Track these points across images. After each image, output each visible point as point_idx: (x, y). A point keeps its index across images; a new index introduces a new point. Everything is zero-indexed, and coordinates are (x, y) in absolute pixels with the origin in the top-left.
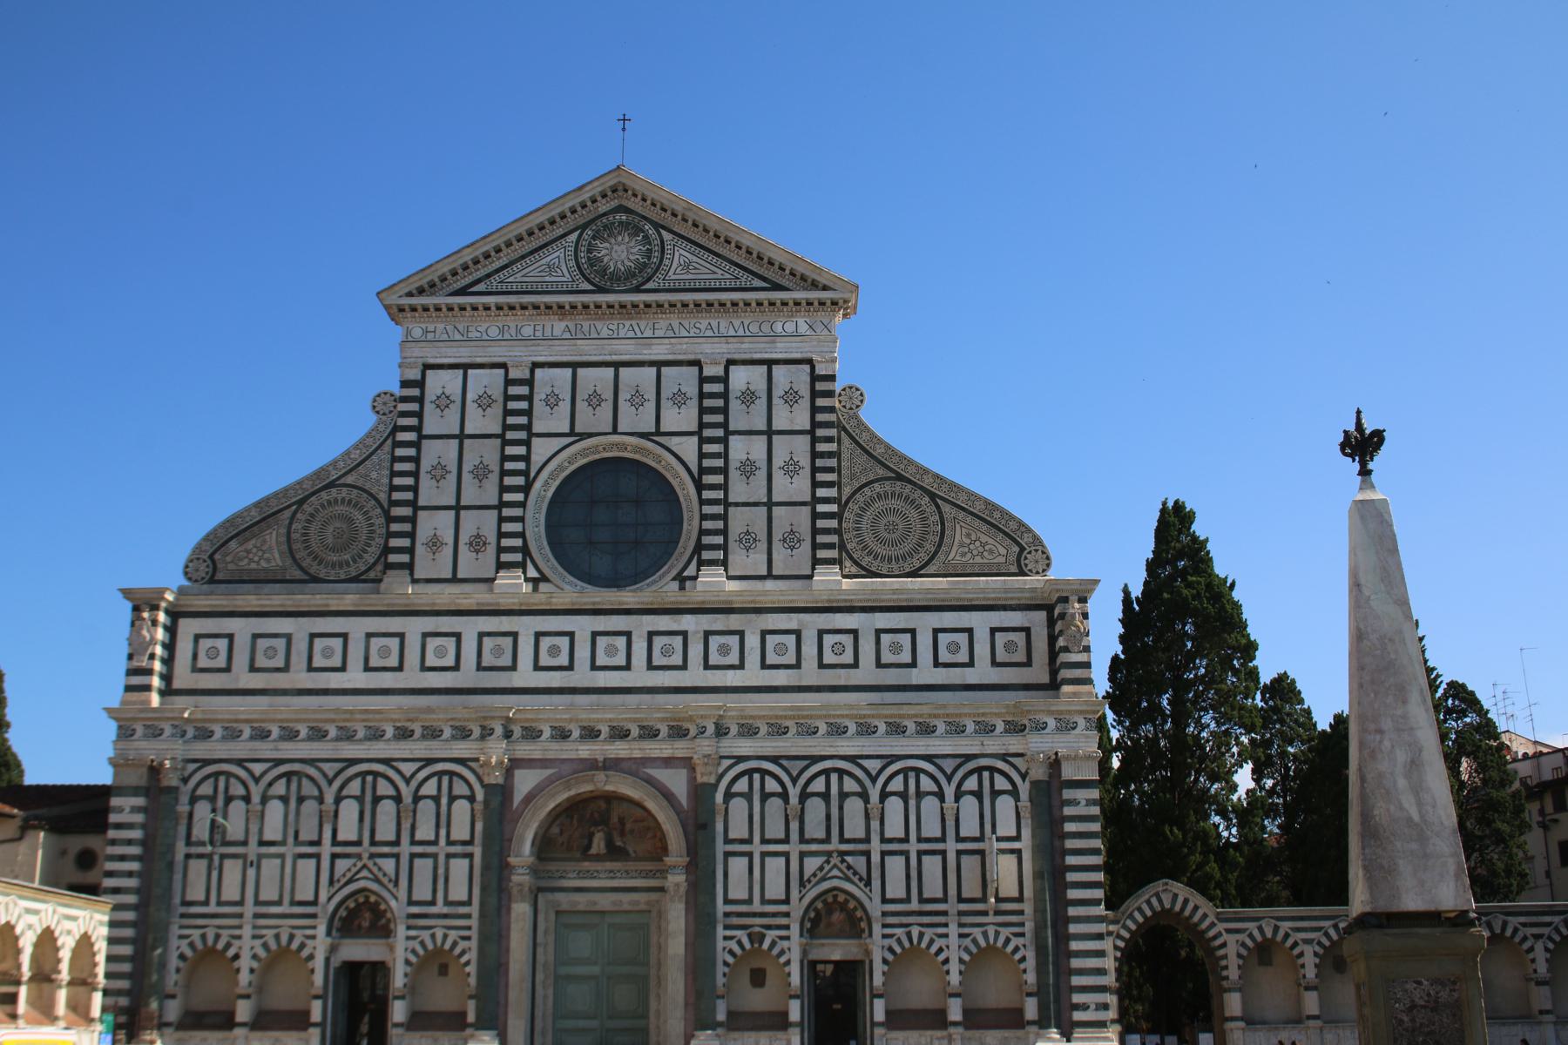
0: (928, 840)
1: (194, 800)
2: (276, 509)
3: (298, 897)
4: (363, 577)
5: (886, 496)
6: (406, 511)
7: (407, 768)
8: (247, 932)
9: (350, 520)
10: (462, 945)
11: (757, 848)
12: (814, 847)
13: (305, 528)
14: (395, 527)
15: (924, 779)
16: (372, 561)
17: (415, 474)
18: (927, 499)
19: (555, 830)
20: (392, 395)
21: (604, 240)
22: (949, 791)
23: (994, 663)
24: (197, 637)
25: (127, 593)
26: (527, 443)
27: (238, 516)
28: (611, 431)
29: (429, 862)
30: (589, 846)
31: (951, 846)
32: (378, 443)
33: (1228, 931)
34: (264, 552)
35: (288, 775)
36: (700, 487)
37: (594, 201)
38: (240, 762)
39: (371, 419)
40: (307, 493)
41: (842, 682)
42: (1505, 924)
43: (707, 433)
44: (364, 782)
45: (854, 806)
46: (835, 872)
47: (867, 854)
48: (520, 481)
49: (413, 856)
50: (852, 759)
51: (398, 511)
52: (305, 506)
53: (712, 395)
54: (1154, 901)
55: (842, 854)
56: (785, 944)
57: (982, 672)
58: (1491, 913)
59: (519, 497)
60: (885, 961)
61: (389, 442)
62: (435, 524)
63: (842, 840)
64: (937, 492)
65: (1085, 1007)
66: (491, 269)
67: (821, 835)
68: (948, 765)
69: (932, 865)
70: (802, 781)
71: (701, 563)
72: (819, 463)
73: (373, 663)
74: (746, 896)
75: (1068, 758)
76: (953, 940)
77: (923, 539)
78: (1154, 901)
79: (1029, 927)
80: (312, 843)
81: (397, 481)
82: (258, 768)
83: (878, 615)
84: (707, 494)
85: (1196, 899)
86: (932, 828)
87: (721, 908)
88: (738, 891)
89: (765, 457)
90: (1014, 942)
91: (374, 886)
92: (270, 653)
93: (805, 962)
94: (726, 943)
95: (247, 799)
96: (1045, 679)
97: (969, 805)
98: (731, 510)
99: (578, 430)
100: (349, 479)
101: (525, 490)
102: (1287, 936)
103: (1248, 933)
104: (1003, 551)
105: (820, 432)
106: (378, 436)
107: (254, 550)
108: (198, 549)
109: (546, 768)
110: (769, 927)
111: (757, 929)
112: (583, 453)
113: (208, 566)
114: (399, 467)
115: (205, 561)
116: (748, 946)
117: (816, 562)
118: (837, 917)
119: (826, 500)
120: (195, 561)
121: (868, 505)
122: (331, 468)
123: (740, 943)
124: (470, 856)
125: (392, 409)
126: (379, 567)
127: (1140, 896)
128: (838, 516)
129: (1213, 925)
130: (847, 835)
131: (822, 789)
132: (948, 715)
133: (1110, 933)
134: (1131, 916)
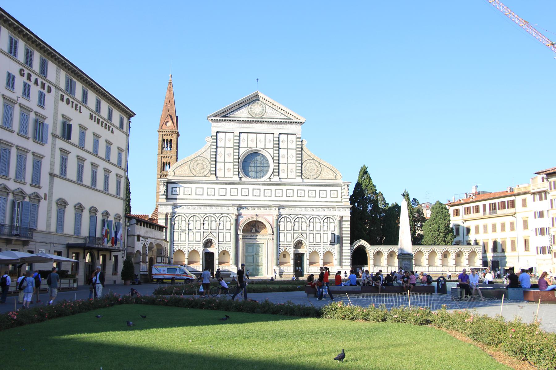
0: (318, 231)
3: (196, 240)
7: (218, 215)
9: (202, 164)
10: (229, 249)
11: (285, 232)
12: (296, 232)
13: (193, 165)
14: (212, 166)
19: (245, 227)
21: (253, 106)
22: (322, 222)
24: (172, 188)
29: (223, 233)
30: (252, 231)
31: (322, 232)
33: (372, 249)
38: (184, 213)
43: (275, 149)
44: (209, 218)
45: (304, 224)
46: (300, 237)
47: (306, 233)
50: (304, 215)
51: (212, 163)
53: (276, 141)
60: (309, 253)
63: (302, 231)
66: (230, 112)
67: (298, 230)
68: (322, 217)
69: (318, 235)
72: (297, 156)
73: (209, 194)
74: (283, 241)
80: (199, 230)
81: (212, 156)
82: (187, 215)
84: (275, 161)
85: (366, 243)
86: (318, 229)
88: (282, 239)
90: (333, 250)
92: (188, 191)
95: (185, 221)
96: (340, 201)
97: (325, 224)
98: (280, 165)
99: (249, 147)
100: (202, 155)
101: (239, 159)
102: (382, 250)
105: (297, 149)
110: (288, 247)
112: (249, 151)
118: (300, 245)
119: (298, 163)
121: (307, 164)
124: (230, 232)
126: (209, 174)
130: (302, 230)
131: (298, 221)
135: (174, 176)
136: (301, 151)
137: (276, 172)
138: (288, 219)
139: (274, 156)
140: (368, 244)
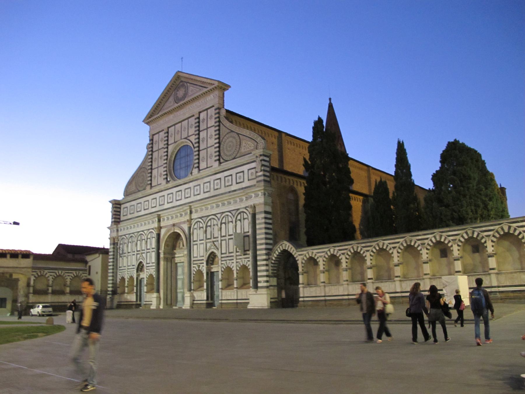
1: (120, 244)
5: (229, 138)
8: (126, 273)
9: (143, 176)
15: (230, 218)
17: (152, 162)
18: (237, 135)
21: (178, 91)
23: (249, 180)
25: (110, 202)
26: (167, 148)
27: (130, 180)
28: (180, 139)
33: (300, 255)
35: (131, 237)
36: (194, 148)
37: (175, 82)
38: (125, 235)
41: (218, 193)
42: (384, 244)
46: (212, 247)
47: (218, 241)
48: (166, 157)
49: (147, 252)
50: (214, 215)
54: (281, 247)
55: (213, 242)
56: (203, 267)
57: (246, 184)
58: (378, 241)
59: (165, 161)
62: (155, 172)
64: (239, 133)
65: (260, 282)
70: (206, 223)
71: (195, 168)
75: (257, 205)
76: (234, 264)
77: (236, 147)
78: (281, 247)
79: (251, 258)
82: (127, 236)
83: (225, 172)
85: (291, 246)
87: (192, 259)
89: (206, 135)
90: (249, 263)
91: (141, 260)
93: (209, 273)
94: (194, 268)
97: (238, 222)
98: (201, 152)
99: (176, 141)
100: (143, 167)
102: (316, 255)
103: (304, 255)
104: (253, 145)
109: (165, 228)
111: (199, 264)
116: (197, 269)
117: (216, 161)
121: (225, 141)
123: (196, 268)
127: (277, 246)
128: (219, 147)
129: (295, 253)
132: (233, 198)
133: (269, 259)
134: (275, 252)
136: (219, 126)
137: (196, 163)
138: (200, 223)
139: (196, 143)
140: (293, 248)
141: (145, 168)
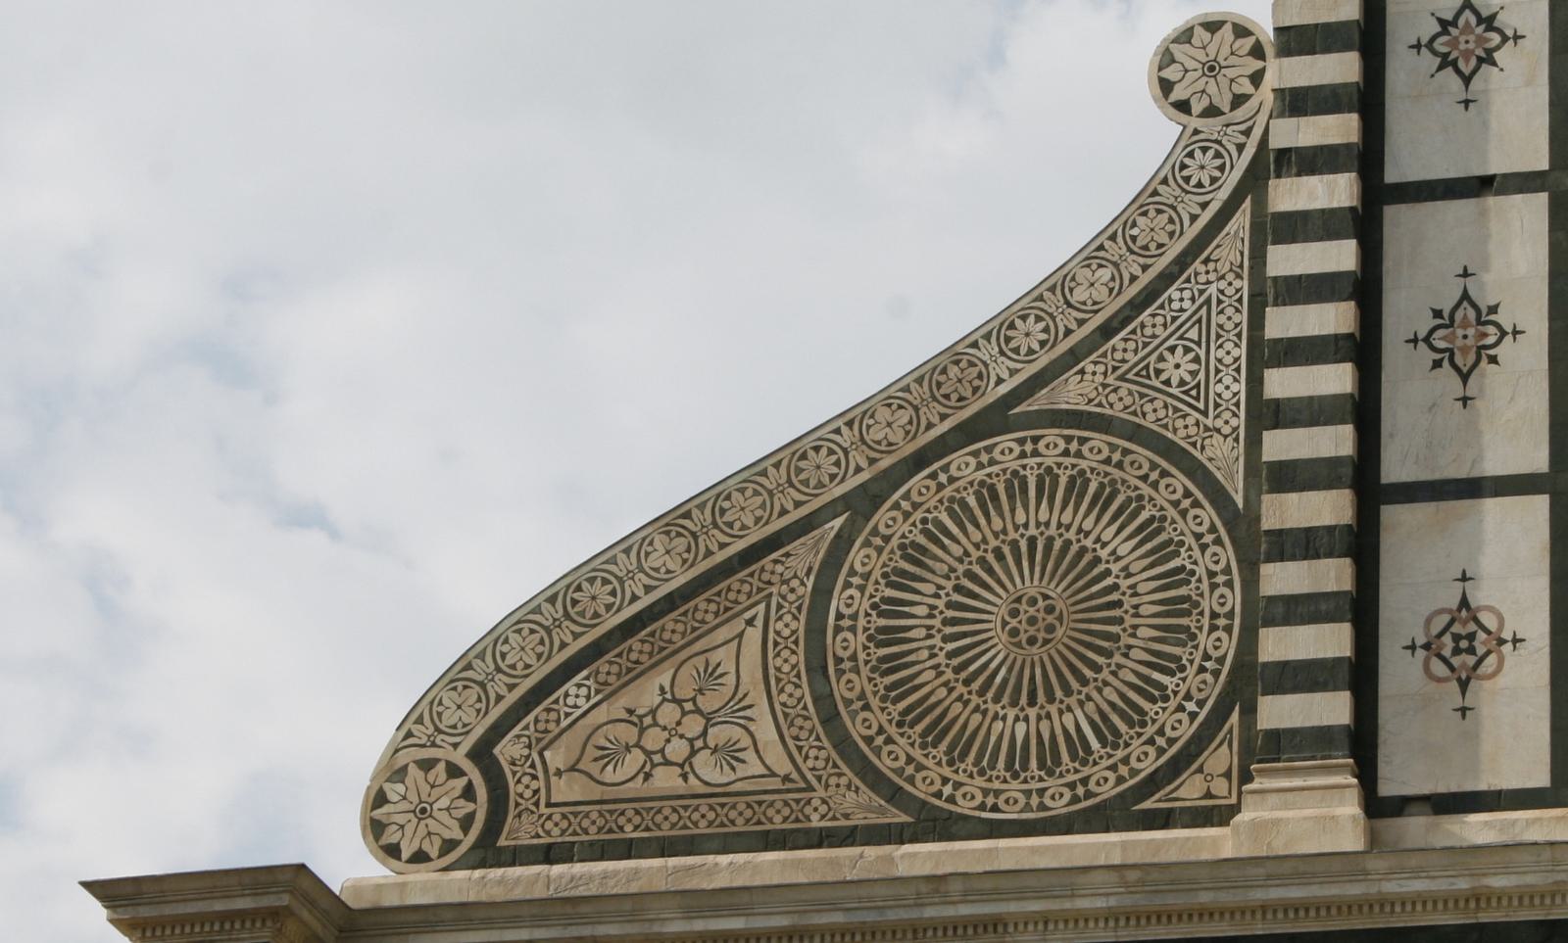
2: (754, 537)
4: (1148, 804)
6: (1331, 508)
9: (1080, 565)
14: (1283, 578)
16: (1186, 731)
20: (1241, 31)
27: (596, 571)
32: (1192, 232)
34: (709, 720)
39: (1161, 133)
40: (886, 462)
52: (882, 516)
61: (1241, 222)
81: (1282, 383)
100: (1072, 393)
106: (1191, 204)
107: (669, 714)
108: (421, 720)
113: (468, 793)
114: (1285, 322)
115: (454, 771)
120: (414, 772)
122: (988, 351)
125: (1248, 88)
126: (1220, 758)
135: (488, 852)
141: (1137, 434)
